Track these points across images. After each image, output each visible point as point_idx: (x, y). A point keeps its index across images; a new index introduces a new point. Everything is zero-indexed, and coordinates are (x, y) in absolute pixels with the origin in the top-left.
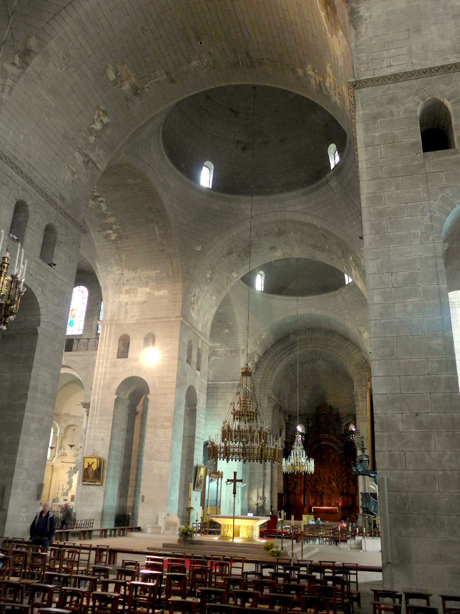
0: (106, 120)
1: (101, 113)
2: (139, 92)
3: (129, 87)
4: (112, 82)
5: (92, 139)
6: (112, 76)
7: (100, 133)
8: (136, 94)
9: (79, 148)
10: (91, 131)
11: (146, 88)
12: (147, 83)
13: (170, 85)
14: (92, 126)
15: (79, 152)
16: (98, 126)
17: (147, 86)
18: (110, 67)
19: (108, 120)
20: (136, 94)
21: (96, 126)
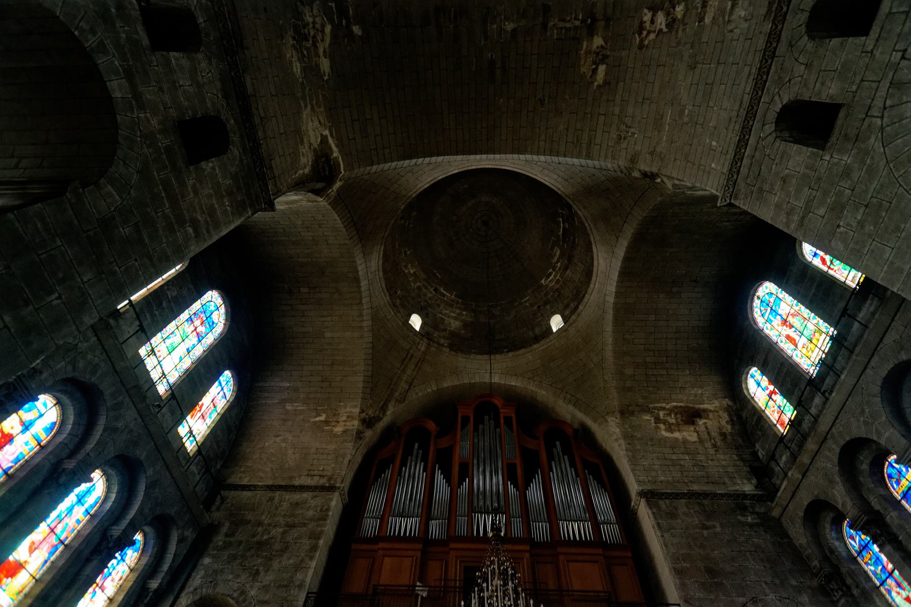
0: (647, 17)
1: (645, 33)
3: (595, 37)
5: (679, 9)
8: (594, 20)
9: (700, 22)
11: (578, 20)
13: (550, 3)
14: (665, 30)
17: (577, 23)
18: (596, 84)
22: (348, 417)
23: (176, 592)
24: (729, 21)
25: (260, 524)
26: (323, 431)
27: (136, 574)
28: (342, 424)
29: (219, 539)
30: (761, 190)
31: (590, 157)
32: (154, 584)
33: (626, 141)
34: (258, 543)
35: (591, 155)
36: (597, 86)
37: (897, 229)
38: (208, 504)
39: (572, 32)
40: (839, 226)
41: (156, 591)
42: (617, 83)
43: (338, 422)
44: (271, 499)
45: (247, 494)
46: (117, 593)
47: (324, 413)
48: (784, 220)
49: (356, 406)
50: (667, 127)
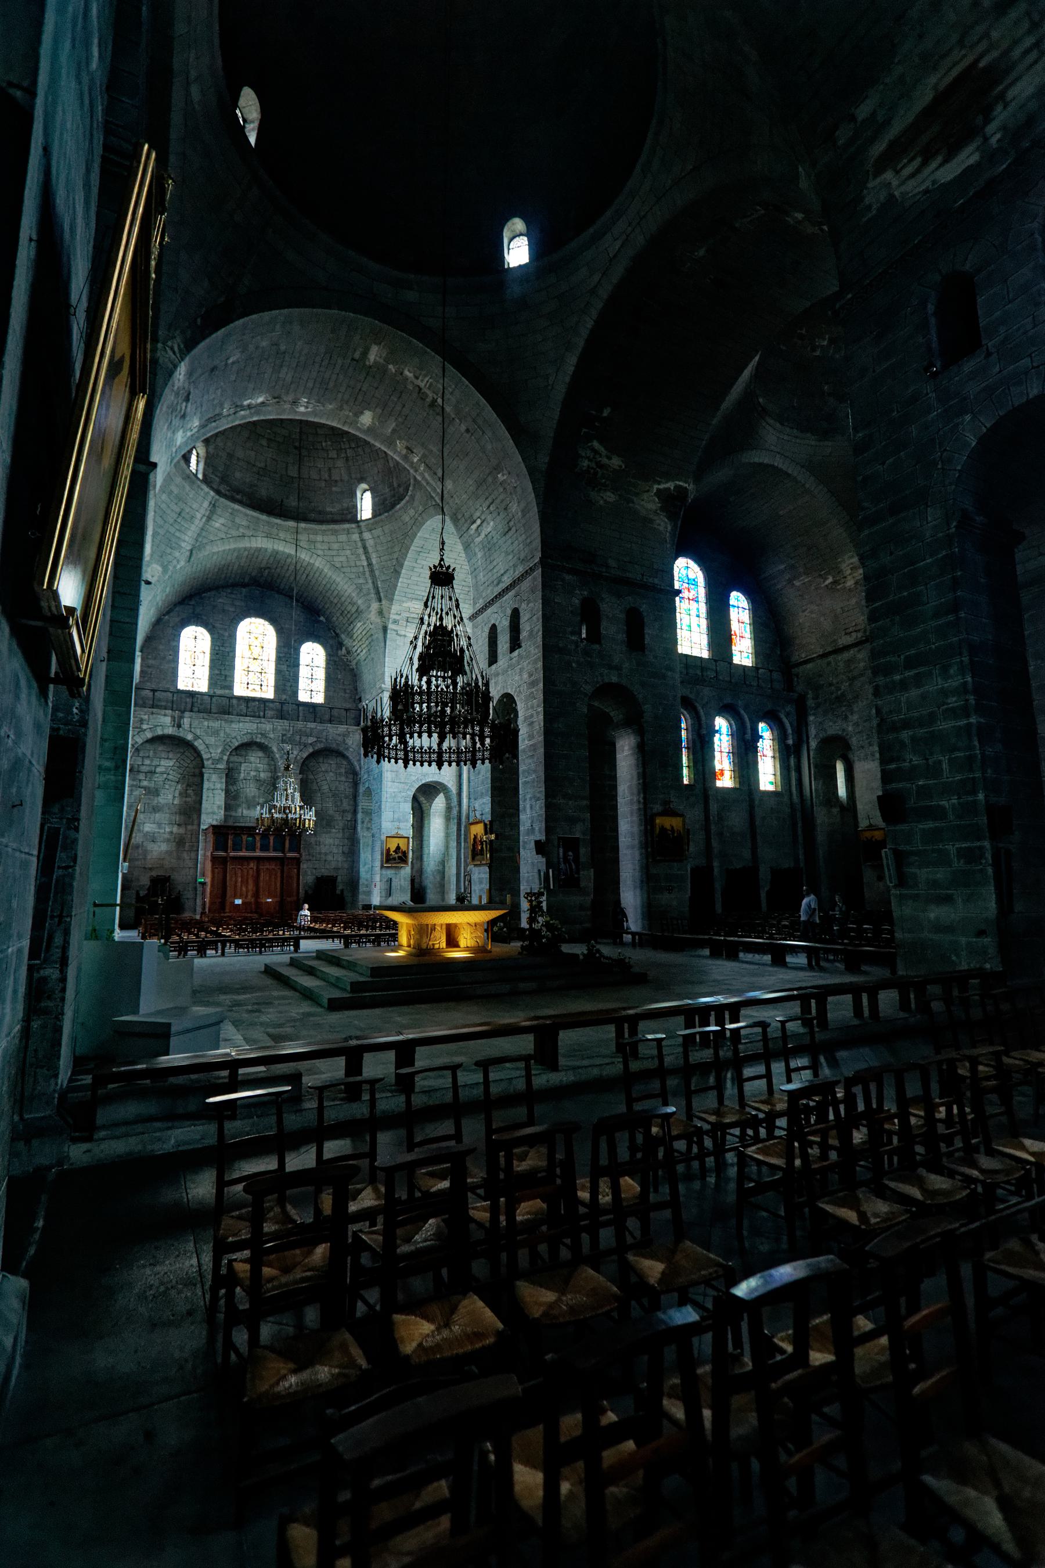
22: (851, 569)
23: (805, 739)
25: (831, 685)
26: (838, 590)
27: (776, 741)
28: (849, 578)
29: (810, 703)
32: (790, 742)
34: (837, 698)
38: (790, 686)
41: (794, 745)
43: (845, 577)
44: (829, 664)
45: (810, 666)
46: (774, 753)
47: (830, 574)
49: (852, 557)
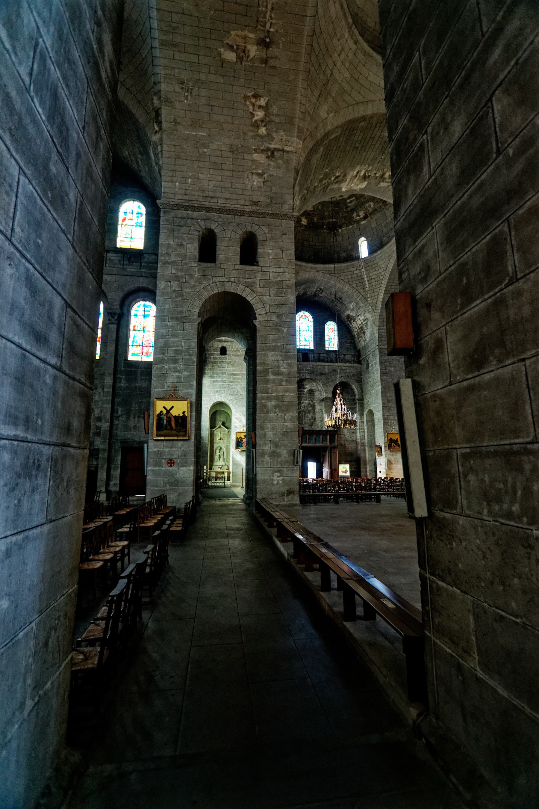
0: (262, 102)
1: (253, 100)
2: (268, 40)
4: (237, 61)
5: (263, 131)
6: (231, 56)
7: (267, 118)
8: (267, 46)
9: (254, 149)
10: (256, 125)
11: (270, 28)
12: (266, 23)
14: (254, 119)
15: (256, 152)
16: (260, 114)
17: (268, 25)
18: (222, 50)
19: (265, 100)
20: (267, 46)
21: (257, 115)
24: (252, 173)
30: (173, 230)
31: (162, 45)
33: (180, 90)
35: (164, 47)
36: (220, 52)
37: (177, 305)
39: (262, 20)
40: (170, 282)
42: (223, 76)
48: (164, 252)
50: (194, 133)
